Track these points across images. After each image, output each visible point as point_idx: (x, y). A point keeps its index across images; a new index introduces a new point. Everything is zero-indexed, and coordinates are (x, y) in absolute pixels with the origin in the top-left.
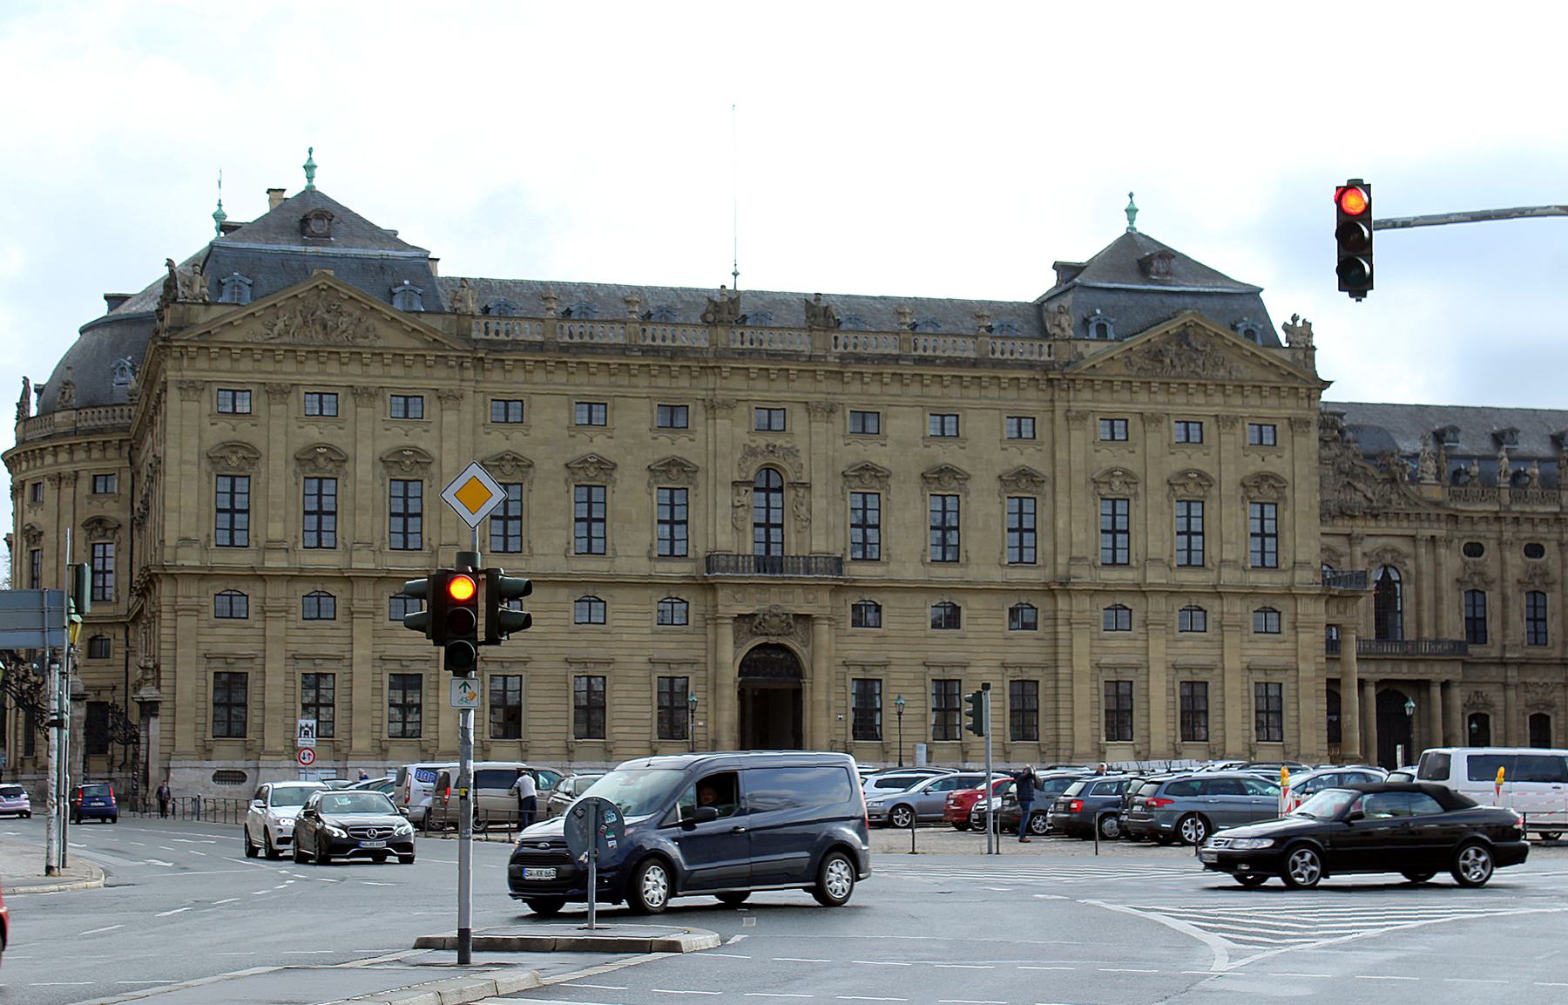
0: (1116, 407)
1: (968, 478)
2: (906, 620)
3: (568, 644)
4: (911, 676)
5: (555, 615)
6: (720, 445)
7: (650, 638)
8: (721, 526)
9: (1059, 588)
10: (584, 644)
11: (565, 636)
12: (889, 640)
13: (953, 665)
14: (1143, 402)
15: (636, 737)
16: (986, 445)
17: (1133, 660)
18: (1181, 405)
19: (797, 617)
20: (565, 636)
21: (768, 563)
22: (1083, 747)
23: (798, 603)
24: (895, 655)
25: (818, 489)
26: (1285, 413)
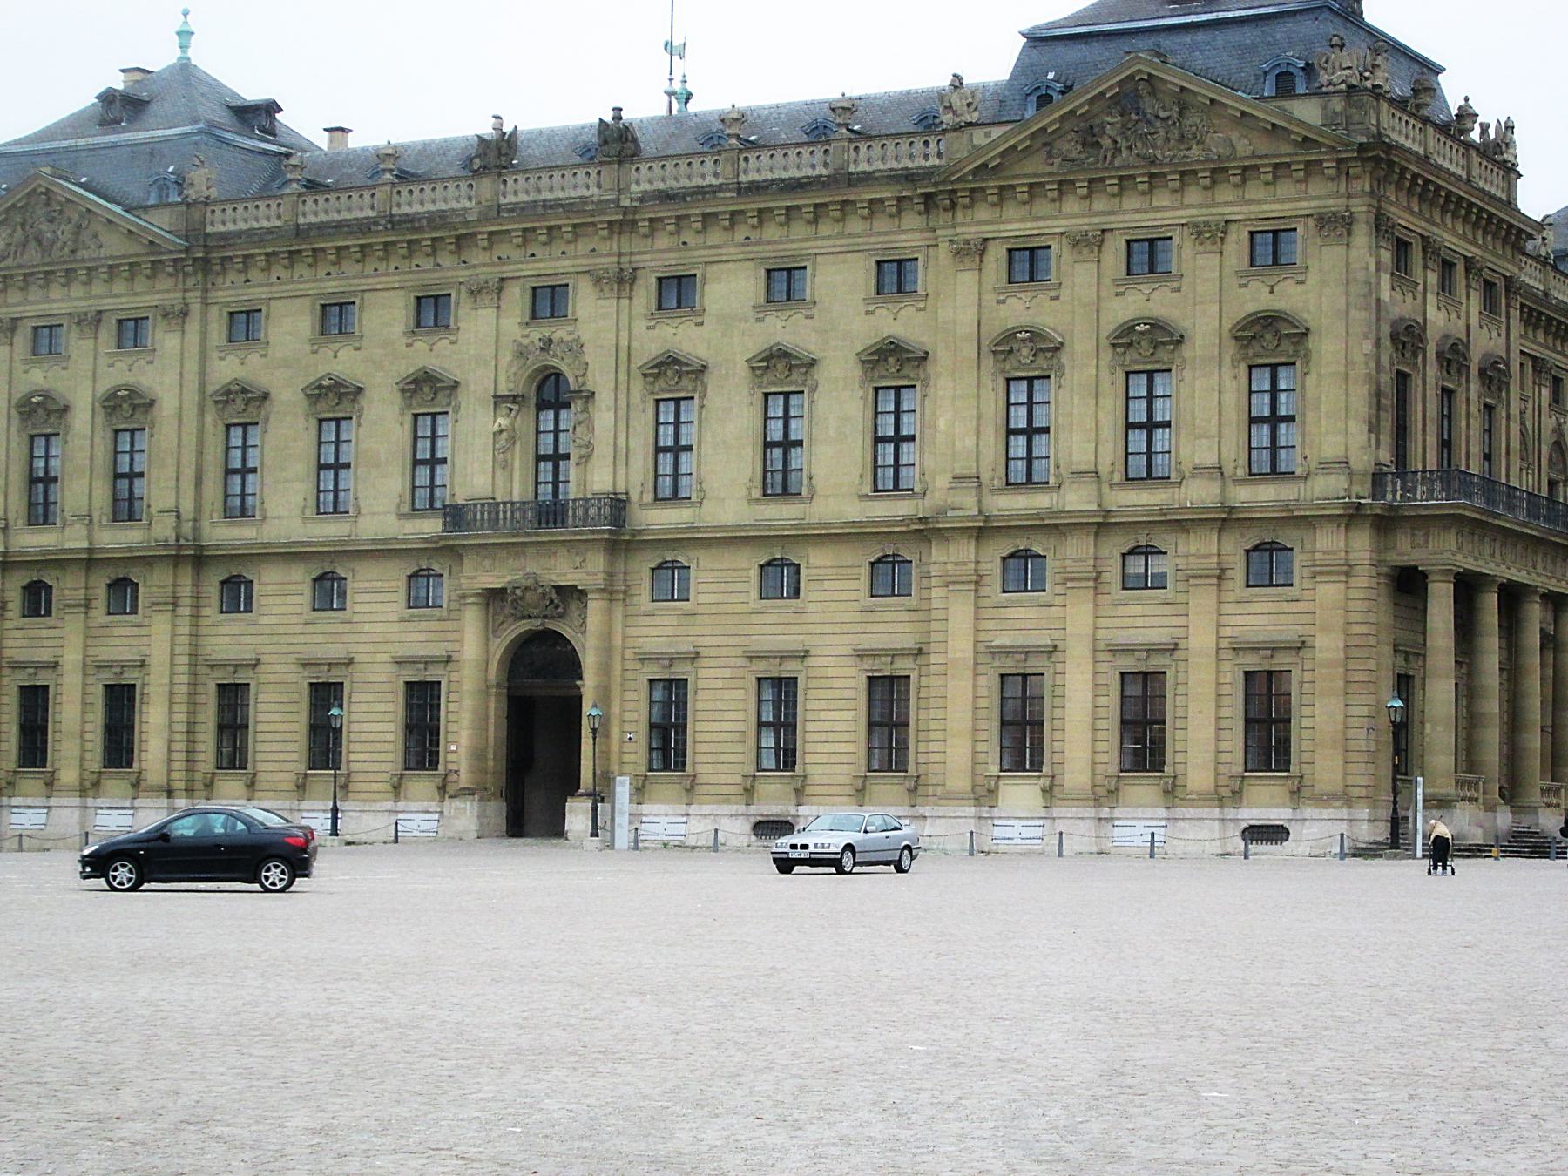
0: (1029, 228)
1: (813, 363)
2: (722, 584)
3: (302, 639)
4: (728, 673)
5: (289, 599)
6: (485, 344)
7: (396, 627)
8: (480, 463)
9: (926, 531)
10: (320, 639)
11: (298, 629)
12: (699, 619)
13: (783, 657)
14: (1072, 215)
15: (377, 767)
16: (842, 310)
17: (1045, 640)
18: (1134, 214)
19: (559, 589)
20: (298, 629)
21: (551, 513)
22: (959, 780)
23: (562, 570)
24: (707, 641)
25: (604, 398)
26: (1306, 206)
